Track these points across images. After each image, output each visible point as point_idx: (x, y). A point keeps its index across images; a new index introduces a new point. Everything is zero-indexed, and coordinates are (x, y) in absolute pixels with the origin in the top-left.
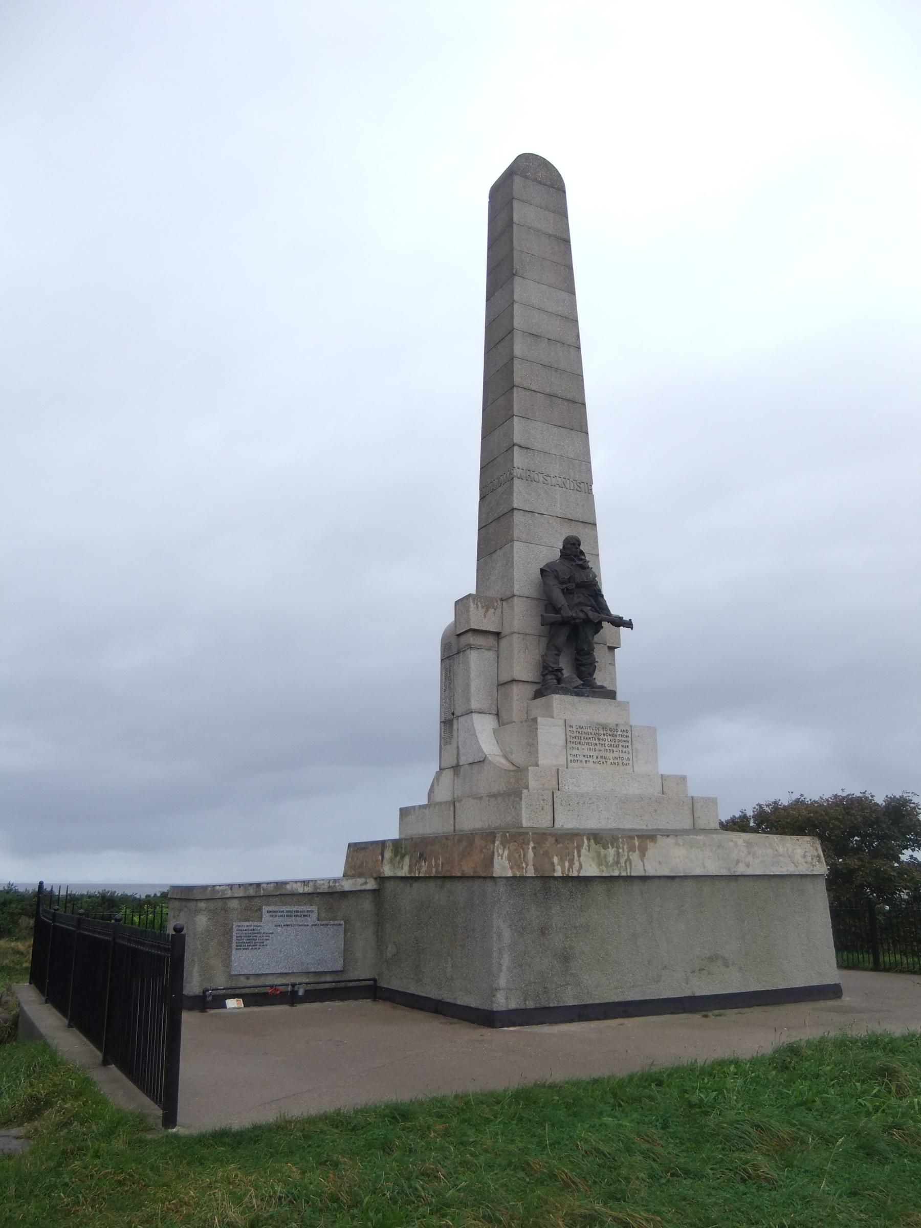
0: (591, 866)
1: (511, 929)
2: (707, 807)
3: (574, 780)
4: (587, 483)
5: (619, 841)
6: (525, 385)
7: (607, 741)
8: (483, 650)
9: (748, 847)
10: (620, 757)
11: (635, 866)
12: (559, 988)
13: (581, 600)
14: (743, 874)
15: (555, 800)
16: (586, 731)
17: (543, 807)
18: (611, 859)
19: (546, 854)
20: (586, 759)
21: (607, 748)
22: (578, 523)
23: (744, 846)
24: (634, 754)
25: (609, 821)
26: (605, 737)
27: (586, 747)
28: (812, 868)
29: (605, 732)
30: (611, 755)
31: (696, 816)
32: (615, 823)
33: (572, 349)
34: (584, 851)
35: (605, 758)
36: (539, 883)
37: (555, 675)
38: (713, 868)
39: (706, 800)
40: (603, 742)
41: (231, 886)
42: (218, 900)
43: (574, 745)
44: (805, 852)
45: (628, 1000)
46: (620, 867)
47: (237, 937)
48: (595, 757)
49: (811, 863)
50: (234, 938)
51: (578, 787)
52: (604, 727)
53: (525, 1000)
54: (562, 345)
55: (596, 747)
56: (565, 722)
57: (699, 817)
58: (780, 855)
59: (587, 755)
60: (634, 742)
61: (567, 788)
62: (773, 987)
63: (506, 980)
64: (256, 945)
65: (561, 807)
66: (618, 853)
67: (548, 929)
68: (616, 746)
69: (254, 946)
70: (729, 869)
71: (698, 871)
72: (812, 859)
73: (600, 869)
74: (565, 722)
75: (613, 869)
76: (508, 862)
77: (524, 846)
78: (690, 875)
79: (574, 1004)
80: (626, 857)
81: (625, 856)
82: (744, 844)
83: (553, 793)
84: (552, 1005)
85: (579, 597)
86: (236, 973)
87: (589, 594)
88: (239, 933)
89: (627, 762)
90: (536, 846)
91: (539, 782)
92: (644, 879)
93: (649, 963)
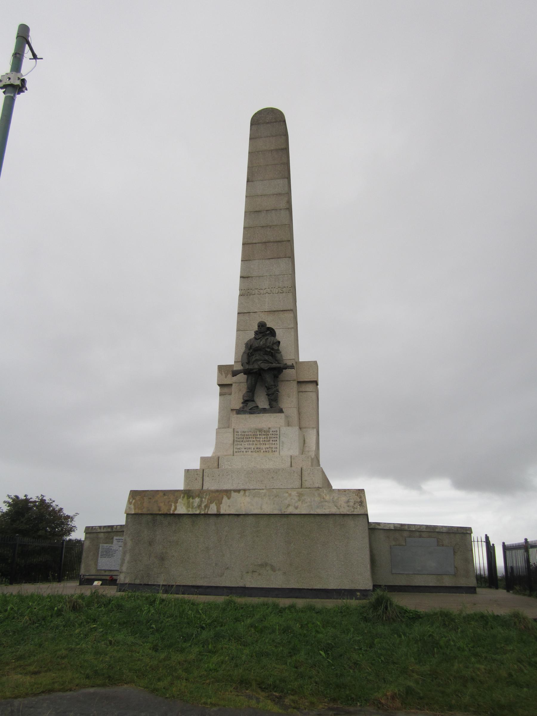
0: (182, 508)
2: (313, 474)
3: (229, 462)
4: (287, 287)
5: (204, 494)
7: (261, 439)
8: (227, 395)
9: (299, 496)
10: (270, 448)
11: (211, 508)
12: (156, 574)
13: (257, 358)
14: (291, 513)
15: (204, 474)
16: (248, 434)
17: (196, 478)
18: (196, 504)
20: (246, 450)
21: (261, 442)
22: (280, 312)
23: (297, 496)
24: (281, 445)
25: (239, 485)
26: (261, 436)
27: (246, 443)
28: (353, 510)
29: (260, 433)
30: (264, 446)
31: (303, 480)
32: (243, 486)
34: (180, 500)
35: (259, 448)
37: (246, 403)
38: (267, 509)
39: (313, 470)
40: (259, 439)
41: (100, 527)
43: (239, 443)
44: (349, 500)
45: (198, 585)
46: (201, 509)
47: (101, 551)
49: (353, 506)
50: (100, 552)
51: (231, 466)
52: (260, 430)
53: (135, 580)
54: (276, 211)
55: (254, 443)
56: (234, 430)
57: (306, 481)
58: (326, 501)
59: (247, 448)
60: (281, 437)
62: (308, 587)
63: (126, 568)
64: (109, 556)
65: (208, 478)
66: (201, 501)
68: (268, 441)
69: (108, 556)
70: (281, 510)
72: (354, 504)
73: (188, 510)
74: (234, 430)
75: (196, 510)
76: (133, 506)
77: (144, 498)
78: (250, 513)
80: (206, 502)
81: (206, 502)
82: (297, 495)
84: (149, 583)
85: (256, 356)
88: (102, 550)
89: (275, 450)
92: (218, 515)
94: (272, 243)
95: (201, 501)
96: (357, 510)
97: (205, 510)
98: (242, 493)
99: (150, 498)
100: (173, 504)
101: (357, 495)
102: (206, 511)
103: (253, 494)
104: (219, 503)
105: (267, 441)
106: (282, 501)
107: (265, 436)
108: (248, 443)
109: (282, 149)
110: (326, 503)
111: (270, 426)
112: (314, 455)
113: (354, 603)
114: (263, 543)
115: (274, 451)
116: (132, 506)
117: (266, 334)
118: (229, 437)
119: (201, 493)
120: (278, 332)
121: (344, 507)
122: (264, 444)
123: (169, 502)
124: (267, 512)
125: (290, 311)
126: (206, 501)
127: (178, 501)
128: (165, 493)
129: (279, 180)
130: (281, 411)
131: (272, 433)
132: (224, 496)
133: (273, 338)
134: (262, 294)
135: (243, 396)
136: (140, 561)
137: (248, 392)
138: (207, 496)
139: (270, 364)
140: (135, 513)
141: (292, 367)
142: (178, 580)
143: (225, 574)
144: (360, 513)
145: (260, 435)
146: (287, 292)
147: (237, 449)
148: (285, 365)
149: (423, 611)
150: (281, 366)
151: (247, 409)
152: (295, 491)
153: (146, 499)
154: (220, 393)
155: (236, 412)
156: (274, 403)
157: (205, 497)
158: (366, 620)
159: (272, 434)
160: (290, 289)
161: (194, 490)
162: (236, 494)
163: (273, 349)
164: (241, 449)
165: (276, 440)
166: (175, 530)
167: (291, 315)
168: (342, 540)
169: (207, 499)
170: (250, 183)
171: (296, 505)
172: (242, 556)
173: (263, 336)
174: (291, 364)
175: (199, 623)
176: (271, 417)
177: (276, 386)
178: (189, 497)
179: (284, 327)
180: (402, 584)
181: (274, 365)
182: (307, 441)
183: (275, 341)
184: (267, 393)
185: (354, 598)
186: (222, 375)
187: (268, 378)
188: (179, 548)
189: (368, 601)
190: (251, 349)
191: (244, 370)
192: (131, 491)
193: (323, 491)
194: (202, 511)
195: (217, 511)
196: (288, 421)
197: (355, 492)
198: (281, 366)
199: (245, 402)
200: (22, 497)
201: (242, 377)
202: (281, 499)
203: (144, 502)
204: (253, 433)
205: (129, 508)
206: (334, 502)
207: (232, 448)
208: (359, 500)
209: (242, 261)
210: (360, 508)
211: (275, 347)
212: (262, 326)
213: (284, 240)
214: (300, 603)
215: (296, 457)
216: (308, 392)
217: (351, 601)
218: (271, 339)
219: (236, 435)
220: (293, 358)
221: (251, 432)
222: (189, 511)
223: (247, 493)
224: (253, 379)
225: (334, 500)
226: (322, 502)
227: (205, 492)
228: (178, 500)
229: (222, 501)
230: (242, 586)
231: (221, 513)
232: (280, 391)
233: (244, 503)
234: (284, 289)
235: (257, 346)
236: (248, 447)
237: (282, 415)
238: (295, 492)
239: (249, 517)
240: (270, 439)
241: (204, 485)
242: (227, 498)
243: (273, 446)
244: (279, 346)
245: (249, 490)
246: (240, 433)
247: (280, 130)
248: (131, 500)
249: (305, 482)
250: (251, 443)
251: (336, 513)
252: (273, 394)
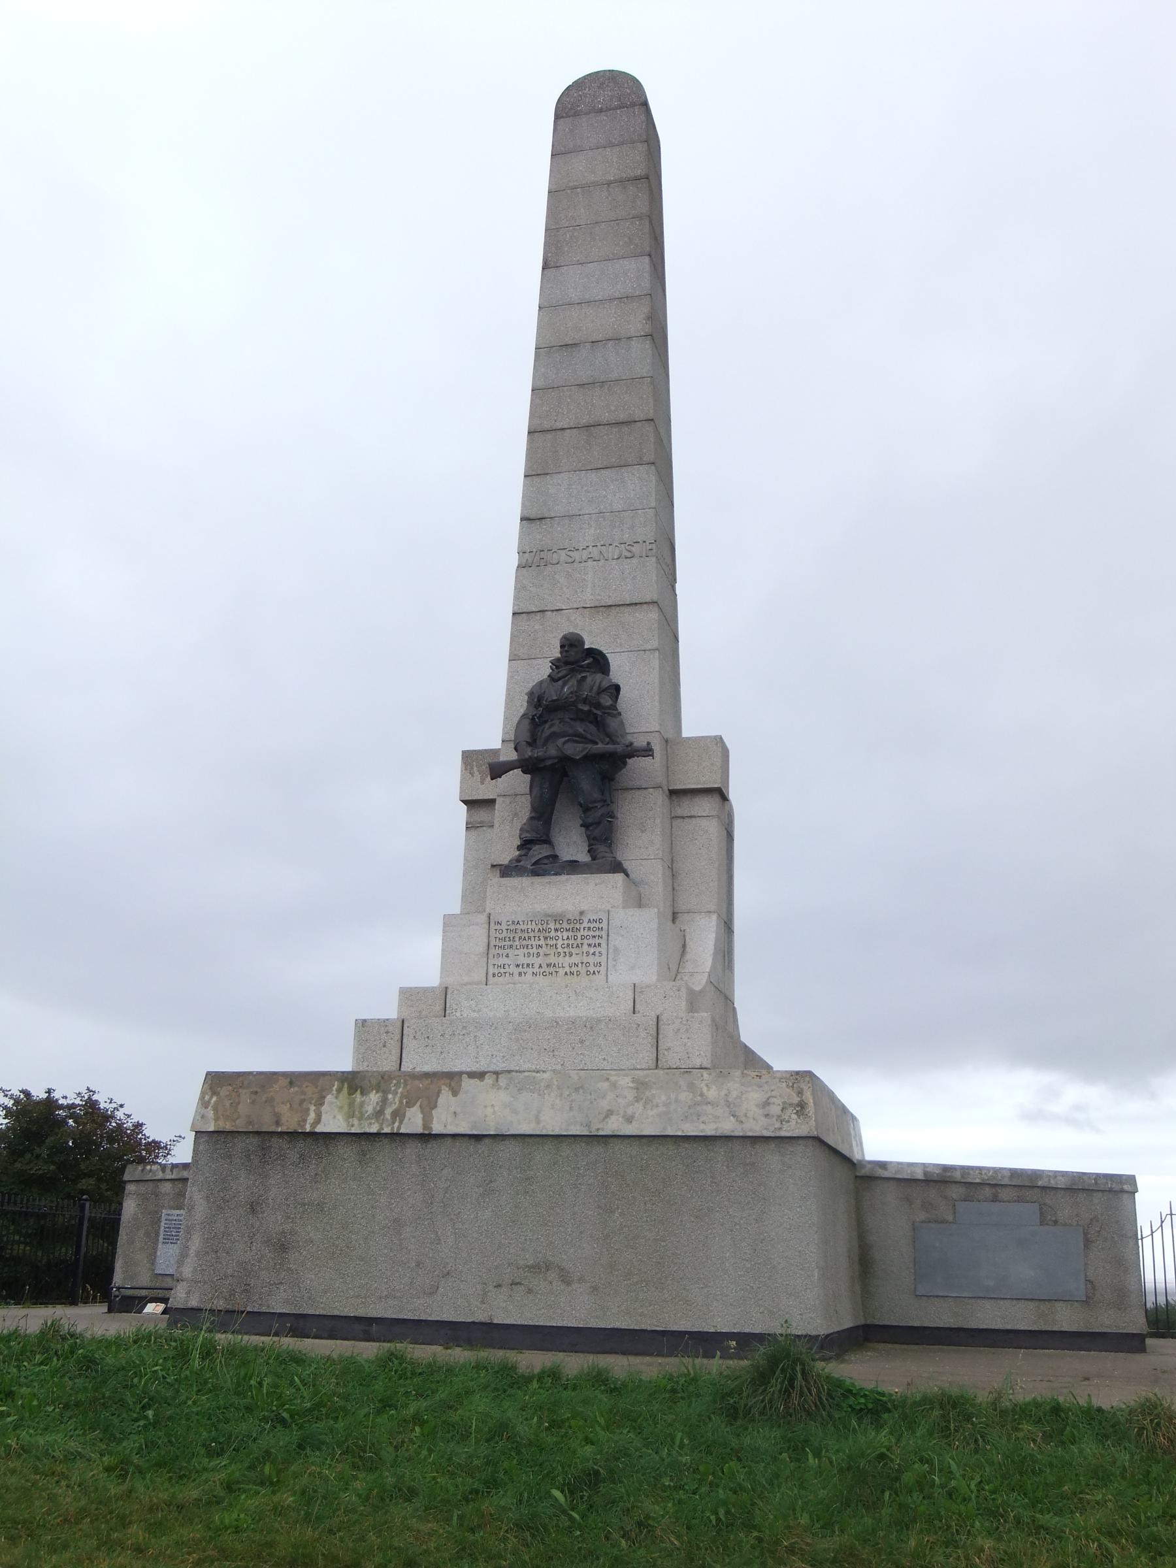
0: (335, 1117)
1: (208, 1201)
2: (687, 1031)
4: (644, 542)
6: (547, 426)
7: (560, 940)
8: (484, 828)
9: (638, 1089)
10: (582, 963)
11: (410, 1119)
14: (616, 1133)
16: (525, 927)
18: (370, 1109)
19: (270, 1101)
20: (520, 969)
21: (560, 950)
25: (494, 1061)
26: (559, 934)
27: (521, 952)
28: (778, 1125)
29: (558, 926)
33: (633, 343)
34: (329, 1098)
35: (554, 966)
36: (254, 1141)
38: (553, 1123)
42: (149, 1182)
43: (500, 951)
44: (768, 1099)
45: (372, 1316)
46: (383, 1119)
48: (536, 966)
49: (779, 1116)
52: (558, 918)
54: (617, 342)
55: (540, 950)
61: (458, 1014)
63: (191, 1269)
66: (384, 1101)
67: (262, 1204)
68: (578, 946)
70: (588, 1126)
71: (526, 1128)
72: (782, 1110)
75: (371, 1124)
77: (240, 1090)
79: (284, 1311)
80: (397, 1105)
81: (395, 1104)
82: (631, 1085)
83: (403, 1021)
86: (160, 1272)
87: (572, 717)
89: (596, 969)
90: (259, 1090)
91: (413, 1009)
92: (426, 1137)
93: (418, 1265)
94: (606, 427)
95: (384, 1101)
96: (790, 1126)
97: (394, 1123)
98: (489, 1080)
99: (256, 1093)
100: (313, 1108)
101: (792, 1087)
102: (397, 1124)
103: (519, 1083)
104: (430, 1105)
106: (592, 1103)
107: (570, 934)
108: (526, 951)
109: (637, 179)
110: (709, 1108)
111: (584, 907)
112: (704, 981)
113: (715, 1365)
114: (541, 1210)
116: (210, 1113)
117: (582, 666)
118: (476, 937)
119: (382, 1082)
120: (615, 662)
121: (754, 1119)
123: (302, 1102)
124: (553, 1131)
125: (651, 606)
126: (397, 1100)
127: (326, 1100)
128: (293, 1079)
129: (625, 262)
130: (617, 867)
132: (443, 1087)
133: (599, 677)
134: (578, 560)
135: (521, 830)
136: (227, 1253)
137: (531, 818)
138: (400, 1088)
139: (589, 746)
140: (217, 1130)
141: (648, 751)
142: (322, 1303)
143: (441, 1290)
144: (796, 1134)
145: (556, 930)
146: (644, 554)
147: (496, 966)
148: (627, 746)
149: (896, 1393)
150: (619, 750)
151: (527, 864)
152: (626, 1075)
153: (245, 1096)
154: (467, 824)
155: (500, 871)
156: (601, 848)
157: (394, 1090)
158: (732, 1414)
159: (589, 928)
160: (650, 547)
161: (367, 1071)
162: (475, 1081)
163: (598, 705)
164: (506, 966)
165: (599, 945)
166: (316, 1174)
167: (653, 615)
168: (748, 1203)
169: (399, 1095)
170: (548, 272)
171: (630, 1111)
172: (485, 1243)
173: (572, 671)
174: (645, 744)
175: (274, 1408)
176: (588, 884)
177: (606, 803)
178: (352, 1090)
179: (632, 649)
180: (942, 1325)
181: (600, 747)
182: (691, 945)
183: (605, 684)
184: (583, 821)
185: (718, 1353)
186: (473, 776)
187: (586, 782)
188: (325, 1221)
189: (746, 1363)
190: (540, 706)
191: (518, 760)
192: (208, 1074)
193: (702, 1076)
194: (384, 1126)
195: (425, 1126)
196: (640, 895)
197: (786, 1078)
198: (619, 748)
199: (526, 845)
200: (39, 1094)
201: (517, 780)
202: (589, 1097)
203: (239, 1103)
204: (540, 926)
205: (203, 1117)
206: (728, 1104)
207: (485, 964)
208: (796, 1100)
209: (525, 476)
210: (799, 1121)
211: (606, 701)
212: (571, 645)
213: (637, 420)
214: (573, 1364)
215: (648, 986)
216: (698, 819)
217: (705, 1361)
218: (594, 679)
220: (657, 729)
221: (533, 923)
222: (353, 1126)
223: (503, 1081)
224: (546, 785)
225: (730, 1100)
226: (697, 1104)
227: (394, 1078)
228: (324, 1097)
229: (437, 1102)
230: (483, 1320)
231: (433, 1133)
232: (619, 815)
233: (492, 1105)
234: (636, 549)
235: (555, 698)
236: (526, 961)
237: (619, 877)
238: (628, 1079)
239: (507, 1142)
241: (403, 1060)
242: (450, 1092)
243: (591, 959)
244: (617, 698)
245: (509, 1072)
246: (504, 927)
247: (632, 129)
248: (207, 1098)
249: (666, 1053)
250: (535, 950)
251: (733, 1134)
252: (599, 823)
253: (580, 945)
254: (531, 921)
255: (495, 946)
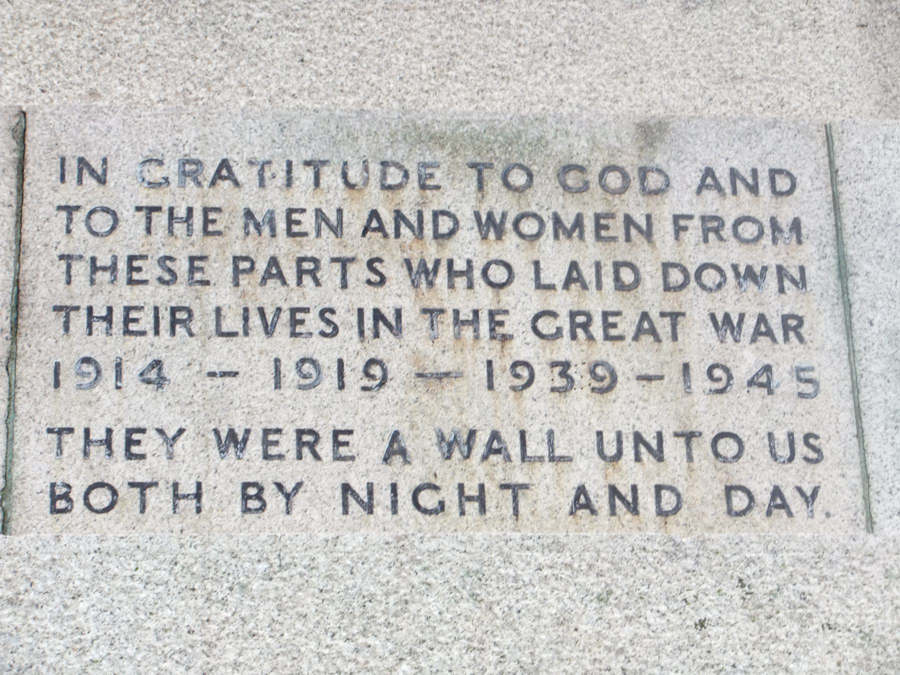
10: (689, 437)
40: (484, 298)
59: (269, 435)
74: (21, 136)
105: (626, 326)
115: (777, 492)
122: (578, 373)
131: (710, 203)
147: (73, 443)
164: (150, 444)
204: (375, 198)
219: (70, 210)
221: (331, 177)
240: (670, 303)
253: (663, 326)
254: (316, 165)
255: (65, 311)
